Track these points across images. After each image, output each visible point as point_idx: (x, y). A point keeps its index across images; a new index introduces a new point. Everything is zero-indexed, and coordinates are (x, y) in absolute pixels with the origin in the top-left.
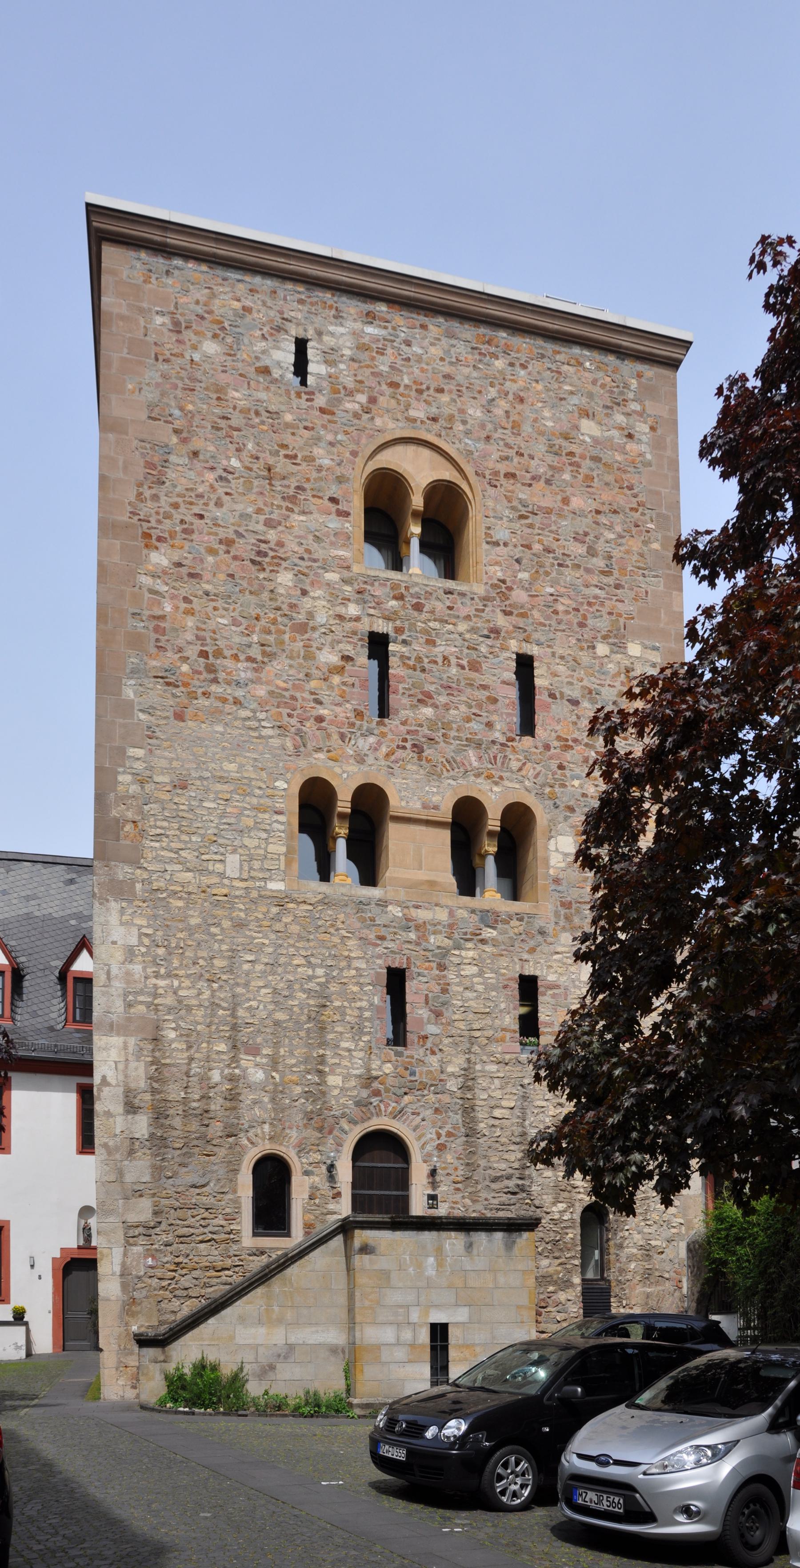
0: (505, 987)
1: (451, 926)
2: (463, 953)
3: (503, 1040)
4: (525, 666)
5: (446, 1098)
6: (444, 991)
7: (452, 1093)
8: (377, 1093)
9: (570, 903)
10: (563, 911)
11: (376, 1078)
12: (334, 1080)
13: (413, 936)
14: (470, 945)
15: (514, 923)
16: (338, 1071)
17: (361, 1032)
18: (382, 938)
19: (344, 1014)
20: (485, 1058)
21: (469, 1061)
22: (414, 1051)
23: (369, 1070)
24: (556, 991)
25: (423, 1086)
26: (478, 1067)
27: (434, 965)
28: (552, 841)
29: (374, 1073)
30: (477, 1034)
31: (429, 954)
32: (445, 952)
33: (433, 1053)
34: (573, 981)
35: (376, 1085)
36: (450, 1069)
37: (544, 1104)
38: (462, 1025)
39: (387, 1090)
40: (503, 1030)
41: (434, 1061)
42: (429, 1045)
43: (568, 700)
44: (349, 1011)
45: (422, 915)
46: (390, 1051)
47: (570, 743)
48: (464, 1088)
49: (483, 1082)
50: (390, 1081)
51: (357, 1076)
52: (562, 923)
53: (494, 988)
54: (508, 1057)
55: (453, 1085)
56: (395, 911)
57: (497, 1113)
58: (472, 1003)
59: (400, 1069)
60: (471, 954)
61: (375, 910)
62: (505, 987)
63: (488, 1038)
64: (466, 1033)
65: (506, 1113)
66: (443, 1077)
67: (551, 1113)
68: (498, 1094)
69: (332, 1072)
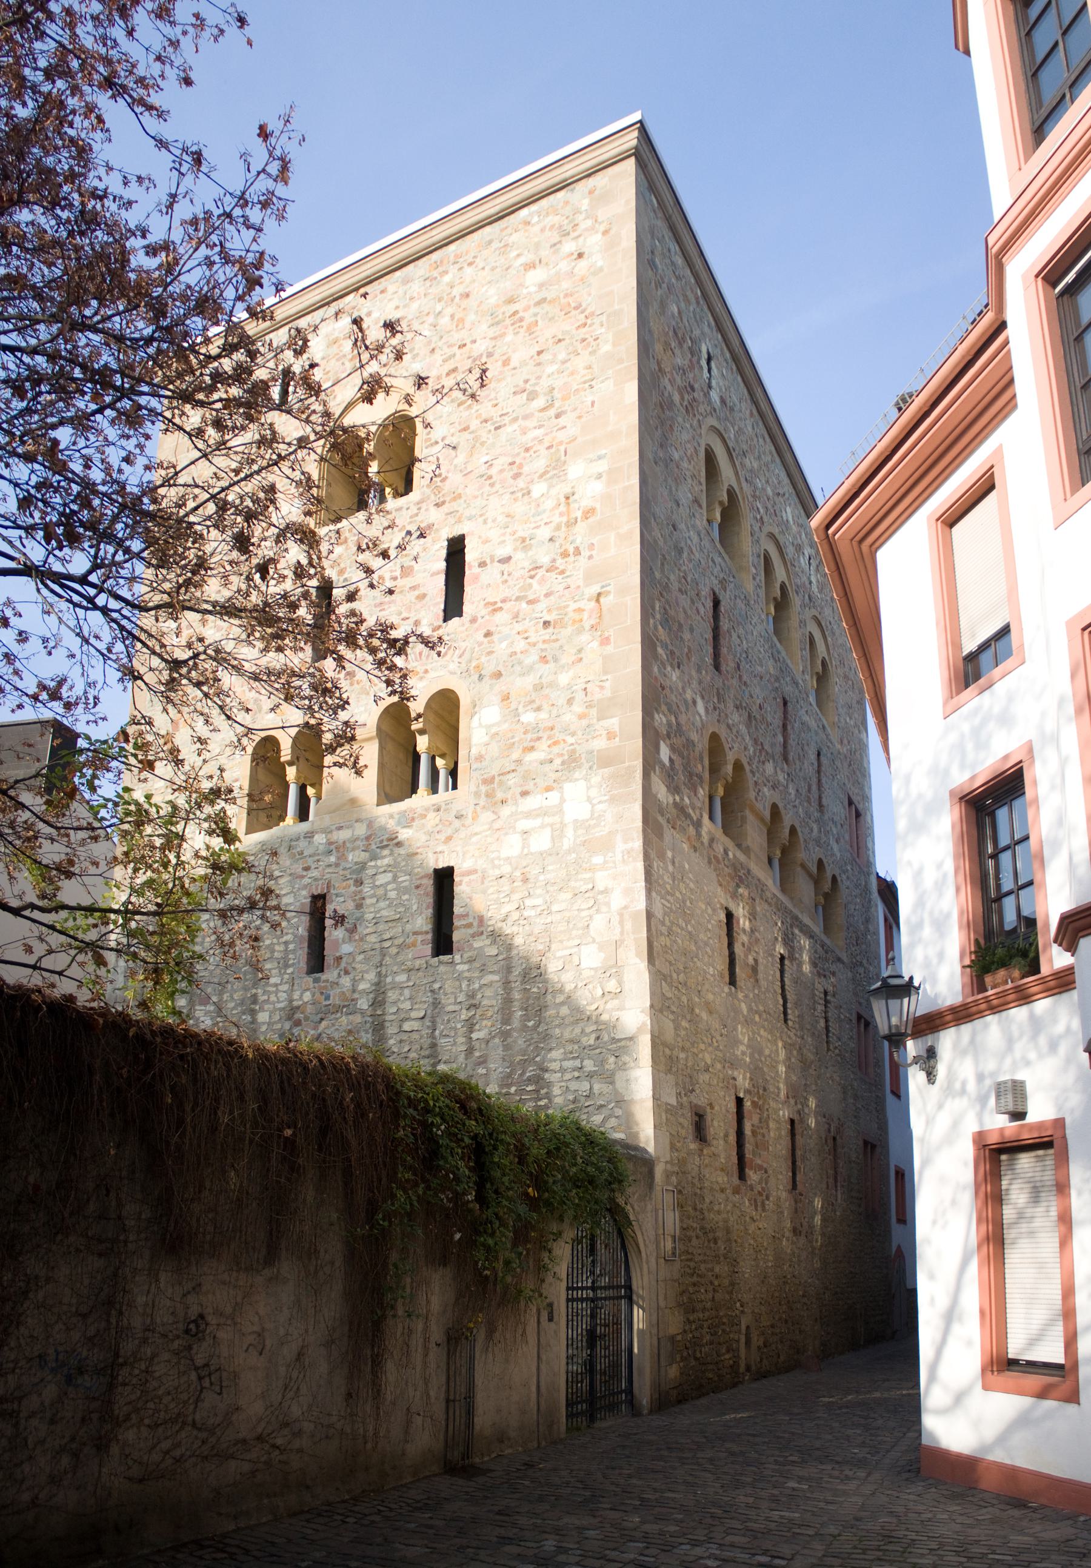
0: (417, 887)
1: (368, 838)
2: (379, 863)
3: (414, 945)
4: (456, 550)
5: (358, 1019)
6: (359, 906)
7: (363, 1013)
8: (298, 1023)
9: (493, 778)
10: (483, 789)
11: (298, 1008)
12: (263, 1017)
13: (333, 859)
14: (386, 852)
15: (431, 815)
16: (266, 1007)
17: (287, 966)
18: (307, 869)
19: (273, 951)
20: (395, 969)
21: (379, 974)
22: (330, 974)
23: (291, 1001)
24: (472, 877)
25: (338, 1009)
26: (389, 980)
27: (351, 882)
28: (476, 718)
29: (295, 1004)
30: (387, 944)
31: (347, 873)
32: (363, 866)
33: (347, 973)
34: (492, 861)
35: (299, 1016)
36: (362, 986)
37: (457, 1008)
38: (373, 939)
39: (307, 1018)
40: (415, 933)
41: (346, 981)
42: (343, 965)
43: (499, 561)
44: (277, 948)
45: (343, 835)
46: (309, 980)
47: (499, 605)
48: (374, 1004)
49: (392, 995)
50: (309, 1009)
51: (281, 1009)
52: (482, 801)
53: (406, 891)
54: (418, 963)
55: (363, 1004)
56: (320, 839)
57: (407, 1026)
58: (384, 913)
59: (318, 995)
60: (386, 861)
61: (302, 844)
62: (417, 887)
63: (399, 946)
64: (377, 946)
65: (415, 1025)
66: (356, 996)
67: (463, 1017)
68: (407, 1005)
69: (262, 1009)
